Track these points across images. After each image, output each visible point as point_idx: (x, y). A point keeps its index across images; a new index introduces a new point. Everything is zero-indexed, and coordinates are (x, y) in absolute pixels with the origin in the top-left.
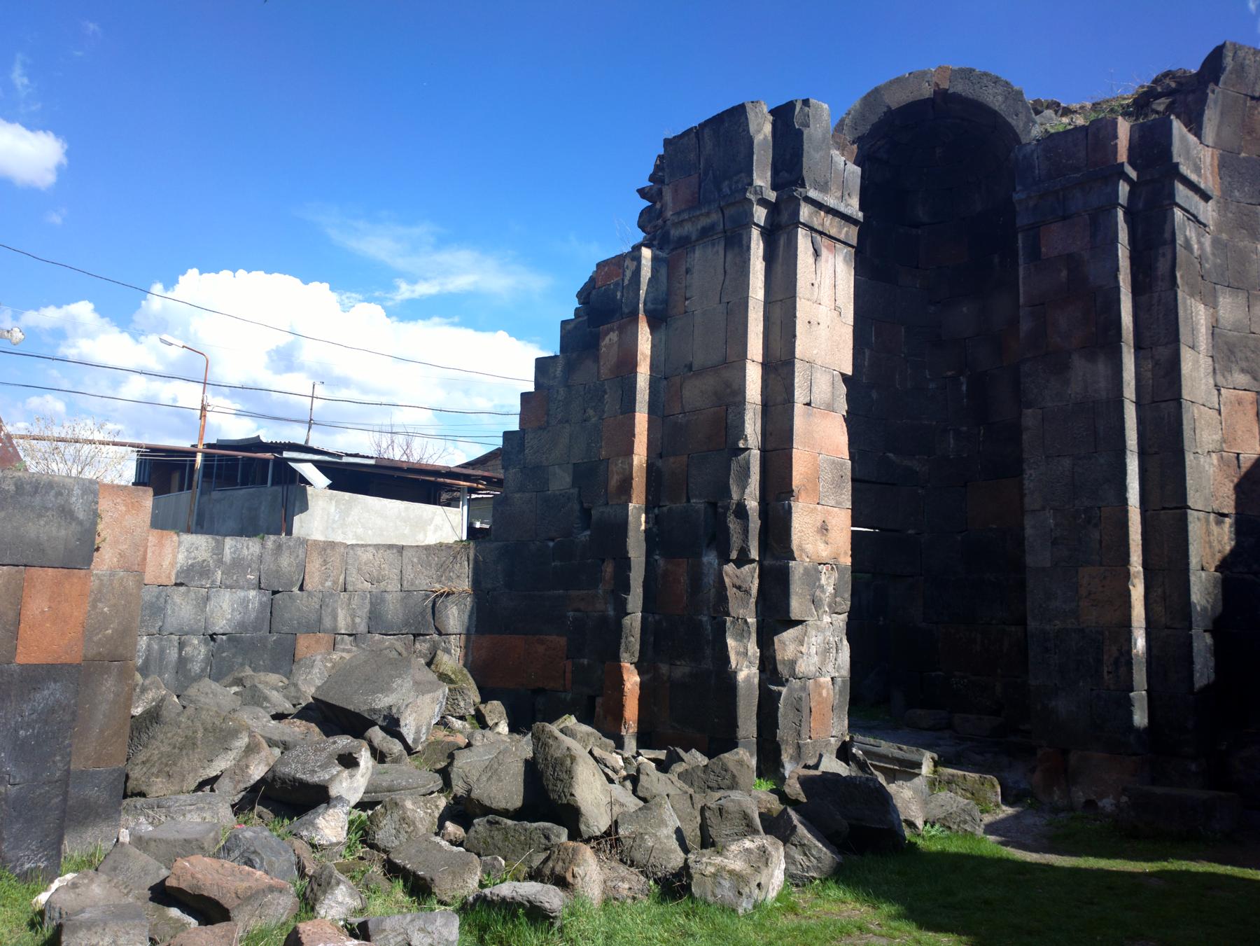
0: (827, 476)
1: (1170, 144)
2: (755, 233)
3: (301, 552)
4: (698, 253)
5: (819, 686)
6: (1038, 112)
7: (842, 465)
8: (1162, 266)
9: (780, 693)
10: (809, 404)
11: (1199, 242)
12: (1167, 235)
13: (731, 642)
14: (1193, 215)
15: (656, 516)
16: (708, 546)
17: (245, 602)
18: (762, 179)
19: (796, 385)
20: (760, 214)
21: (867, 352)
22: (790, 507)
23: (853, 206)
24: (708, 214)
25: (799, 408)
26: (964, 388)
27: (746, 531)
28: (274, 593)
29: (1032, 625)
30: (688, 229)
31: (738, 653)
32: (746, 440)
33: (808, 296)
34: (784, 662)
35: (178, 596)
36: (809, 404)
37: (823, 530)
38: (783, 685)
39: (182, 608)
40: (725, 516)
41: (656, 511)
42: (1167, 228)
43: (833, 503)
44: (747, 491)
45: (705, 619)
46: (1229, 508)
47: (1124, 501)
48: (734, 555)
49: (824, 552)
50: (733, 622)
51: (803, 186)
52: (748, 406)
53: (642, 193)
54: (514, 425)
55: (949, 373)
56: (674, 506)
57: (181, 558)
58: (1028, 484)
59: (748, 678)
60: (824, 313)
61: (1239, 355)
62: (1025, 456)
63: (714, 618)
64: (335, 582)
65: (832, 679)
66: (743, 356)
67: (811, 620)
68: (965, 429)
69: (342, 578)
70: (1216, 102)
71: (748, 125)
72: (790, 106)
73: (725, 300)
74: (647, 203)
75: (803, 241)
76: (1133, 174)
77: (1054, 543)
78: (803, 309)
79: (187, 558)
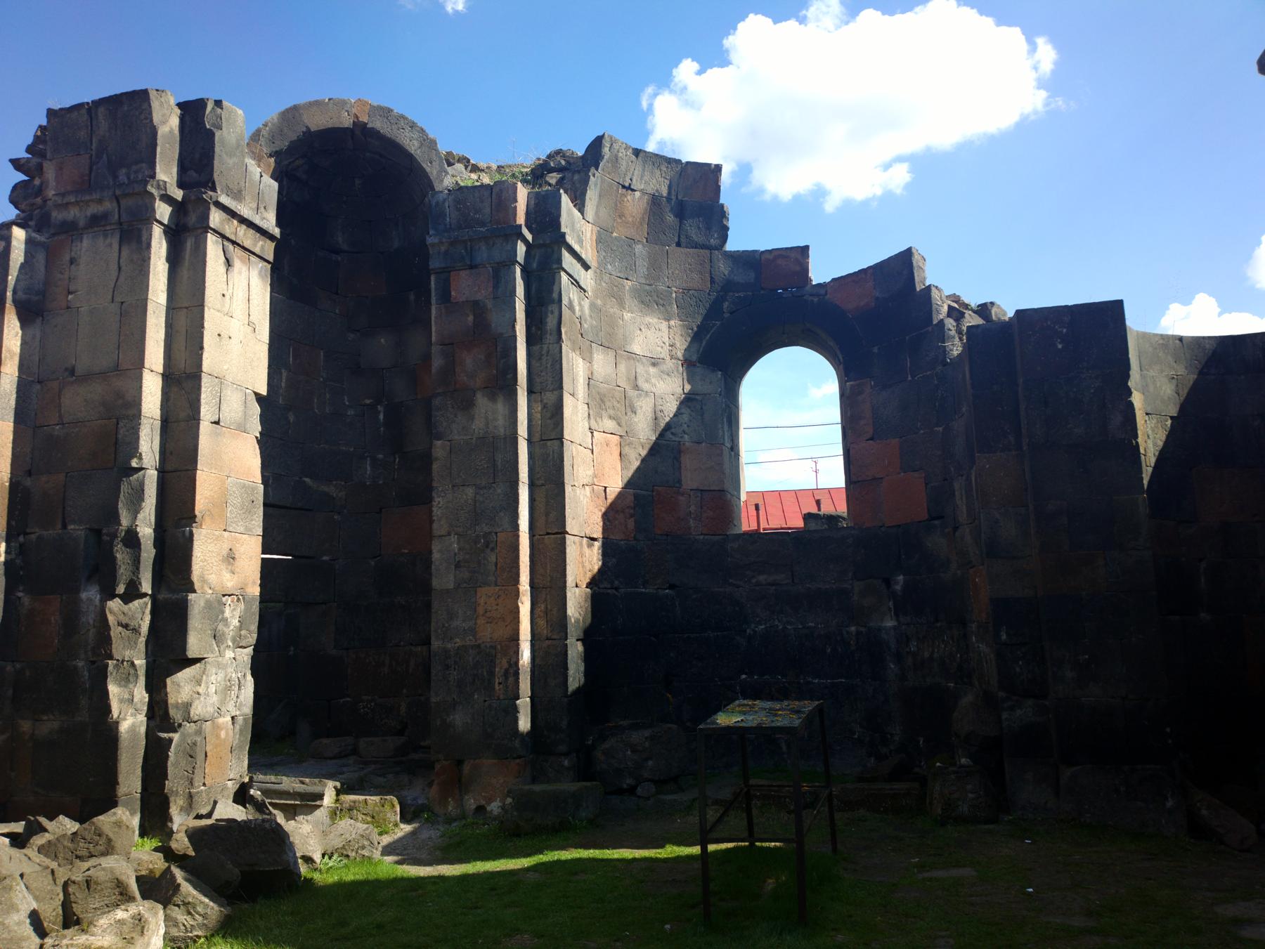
0: (235, 500)
1: (559, 215)
2: (157, 231)
4: (86, 242)
5: (217, 727)
6: (450, 164)
7: (253, 489)
8: (551, 322)
9: (171, 740)
10: (217, 423)
11: (580, 304)
12: (555, 295)
13: (113, 689)
15: (21, 545)
16: (89, 579)
18: (166, 173)
19: (203, 401)
21: (284, 374)
22: (191, 534)
23: (269, 220)
24: (100, 201)
25: (205, 427)
26: (381, 417)
27: (136, 562)
29: (436, 644)
30: (73, 213)
31: (121, 701)
32: (140, 458)
33: (218, 306)
34: (177, 706)
36: (217, 423)
37: (229, 558)
38: (175, 731)
40: (111, 545)
41: (21, 539)
42: (556, 288)
43: (242, 529)
44: (140, 516)
45: (81, 664)
46: (598, 534)
47: (516, 527)
48: (121, 589)
49: (230, 582)
50: (116, 666)
51: (214, 189)
52: (143, 421)
55: (368, 402)
56: (45, 533)
58: (437, 512)
59: (133, 729)
60: (236, 327)
61: (608, 404)
62: (435, 484)
63: (93, 662)
65: (233, 718)
66: (139, 364)
67: (211, 657)
68: (381, 456)
71: (151, 113)
72: (199, 105)
73: (118, 299)
75: (213, 247)
76: (529, 237)
77: (458, 566)
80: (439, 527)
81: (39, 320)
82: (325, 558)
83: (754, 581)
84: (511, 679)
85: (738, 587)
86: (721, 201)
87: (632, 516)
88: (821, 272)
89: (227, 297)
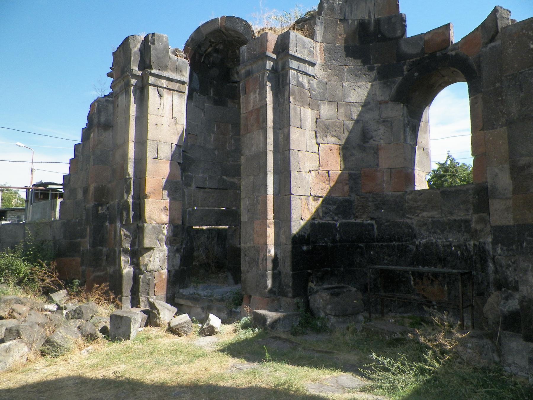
5: (161, 274)
10: (157, 158)
12: (288, 81)
14: (304, 72)
19: (148, 151)
20: (133, 81)
21: (212, 135)
31: (125, 262)
33: (156, 113)
34: (143, 265)
38: (142, 275)
53: (109, 75)
54: (67, 172)
59: (128, 273)
60: (166, 120)
61: (331, 129)
70: (321, 23)
74: (111, 80)
77: (248, 211)
78: (152, 119)
80: (243, 195)
81: (111, 129)
82: (234, 208)
83: (420, 215)
84: (264, 262)
87: (347, 184)
89: (161, 109)
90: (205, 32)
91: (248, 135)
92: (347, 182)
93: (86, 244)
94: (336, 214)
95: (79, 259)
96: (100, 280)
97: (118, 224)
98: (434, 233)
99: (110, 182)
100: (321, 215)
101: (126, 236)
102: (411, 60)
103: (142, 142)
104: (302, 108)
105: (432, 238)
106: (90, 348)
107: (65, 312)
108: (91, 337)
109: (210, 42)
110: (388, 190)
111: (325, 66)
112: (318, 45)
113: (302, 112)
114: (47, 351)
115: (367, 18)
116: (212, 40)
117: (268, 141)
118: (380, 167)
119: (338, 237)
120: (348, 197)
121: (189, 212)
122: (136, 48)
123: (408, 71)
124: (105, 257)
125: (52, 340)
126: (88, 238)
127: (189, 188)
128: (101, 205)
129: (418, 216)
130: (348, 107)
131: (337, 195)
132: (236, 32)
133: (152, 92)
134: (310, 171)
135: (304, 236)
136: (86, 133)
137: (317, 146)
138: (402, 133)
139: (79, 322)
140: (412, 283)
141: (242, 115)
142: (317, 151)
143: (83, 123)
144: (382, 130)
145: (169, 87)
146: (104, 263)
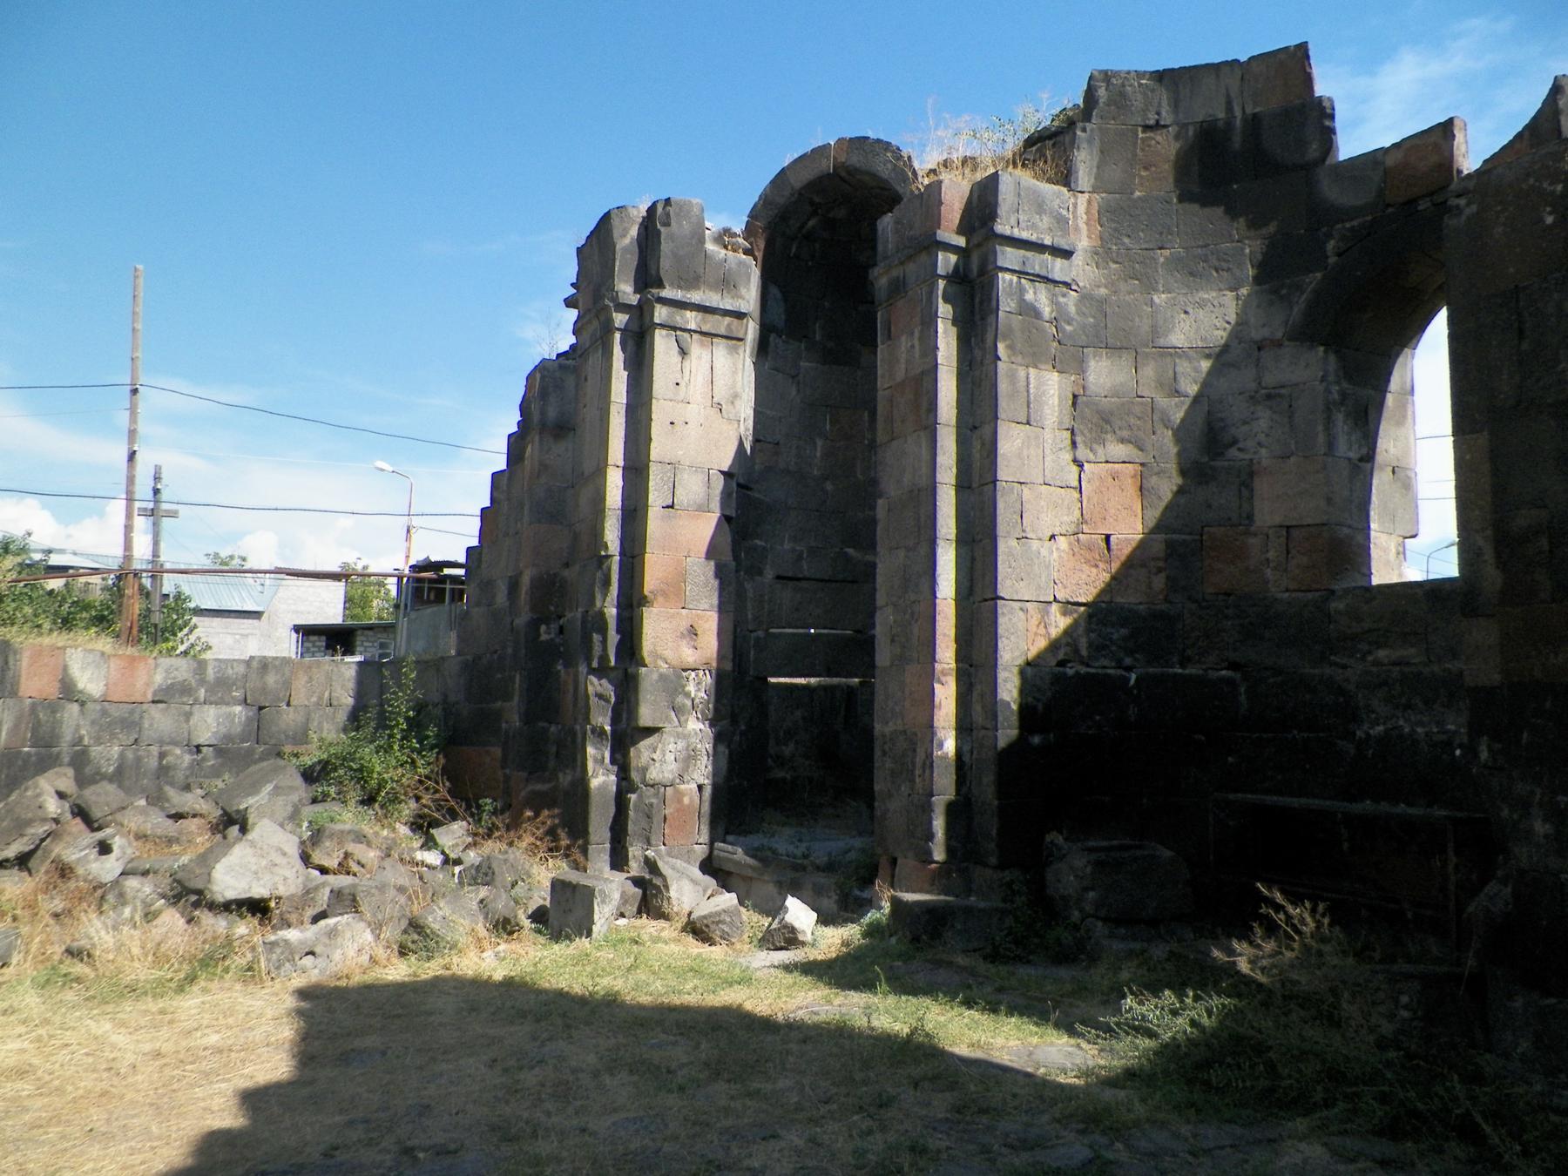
3: (287, 671)
5: (679, 795)
10: (672, 507)
13: (590, 750)
17: (230, 717)
20: (620, 319)
21: (819, 443)
28: (261, 708)
31: (596, 760)
33: (670, 395)
35: (155, 712)
39: (160, 721)
49: (689, 655)
53: (570, 303)
54: (475, 542)
57: (159, 678)
58: (879, 579)
59: (603, 787)
60: (696, 411)
61: (1117, 423)
64: (320, 698)
65: (700, 787)
69: (327, 694)
70: (1090, 141)
74: (573, 314)
77: (893, 641)
78: (660, 412)
79: (166, 678)
80: (881, 599)
81: (571, 434)
83: (1370, 658)
85: (1345, 667)
86: (1318, 93)
87: (1160, 570)
88: (1471, 154)
89: (683, 384)
90: (799, 180)
91: (895, 443)
92: (1161, 564)
93: (512, 713)
94: (1131, 653)
95: (497, 751)
96: (538, 803)
97: (583, 669)
98: (1408, 706)
99: (567, 565)
100: (1084, 653)
101: (600, 696)
102: (1348, 225)
103: (636, 470)
104: (1032, 371)
105: (1401, 722)
106: (503, 947)
107: (457, 869)
108: (505, 927)
109: (812, 203)
110: (1280, 583)
111: (1102, 255)
112: (1082, 200)
113: (1032, 380)
114: (413, 947)
115: (1221, 115)
116: (817, 199)
117: (939, 459)
118: (1258, 523)
119: (1132, 711)
120: (1164, 607)
121: (758, 639)
122: (627, 237)
123: (1339, 255)
124: (554, 749)
125: (421, 922)
126: (516, 699)
127: (758, 578)
128: (547, 621)
129: (1363, 659)
130: (1168, 359)
131: (1132, 600)
132: (874, 176)
133: (663, 344)
134: (1053, 537)
135: (1035, 708)
136: (516, 445)
137: (1075, 469)
138: (1320, 428)
139: (483, 892)
140: (1346, 846)
141: (880, 394)
142: (1076, 484)
143: (510, 421)
144: (1264, 419)
145: (705, 329)
146: (552, 764)
